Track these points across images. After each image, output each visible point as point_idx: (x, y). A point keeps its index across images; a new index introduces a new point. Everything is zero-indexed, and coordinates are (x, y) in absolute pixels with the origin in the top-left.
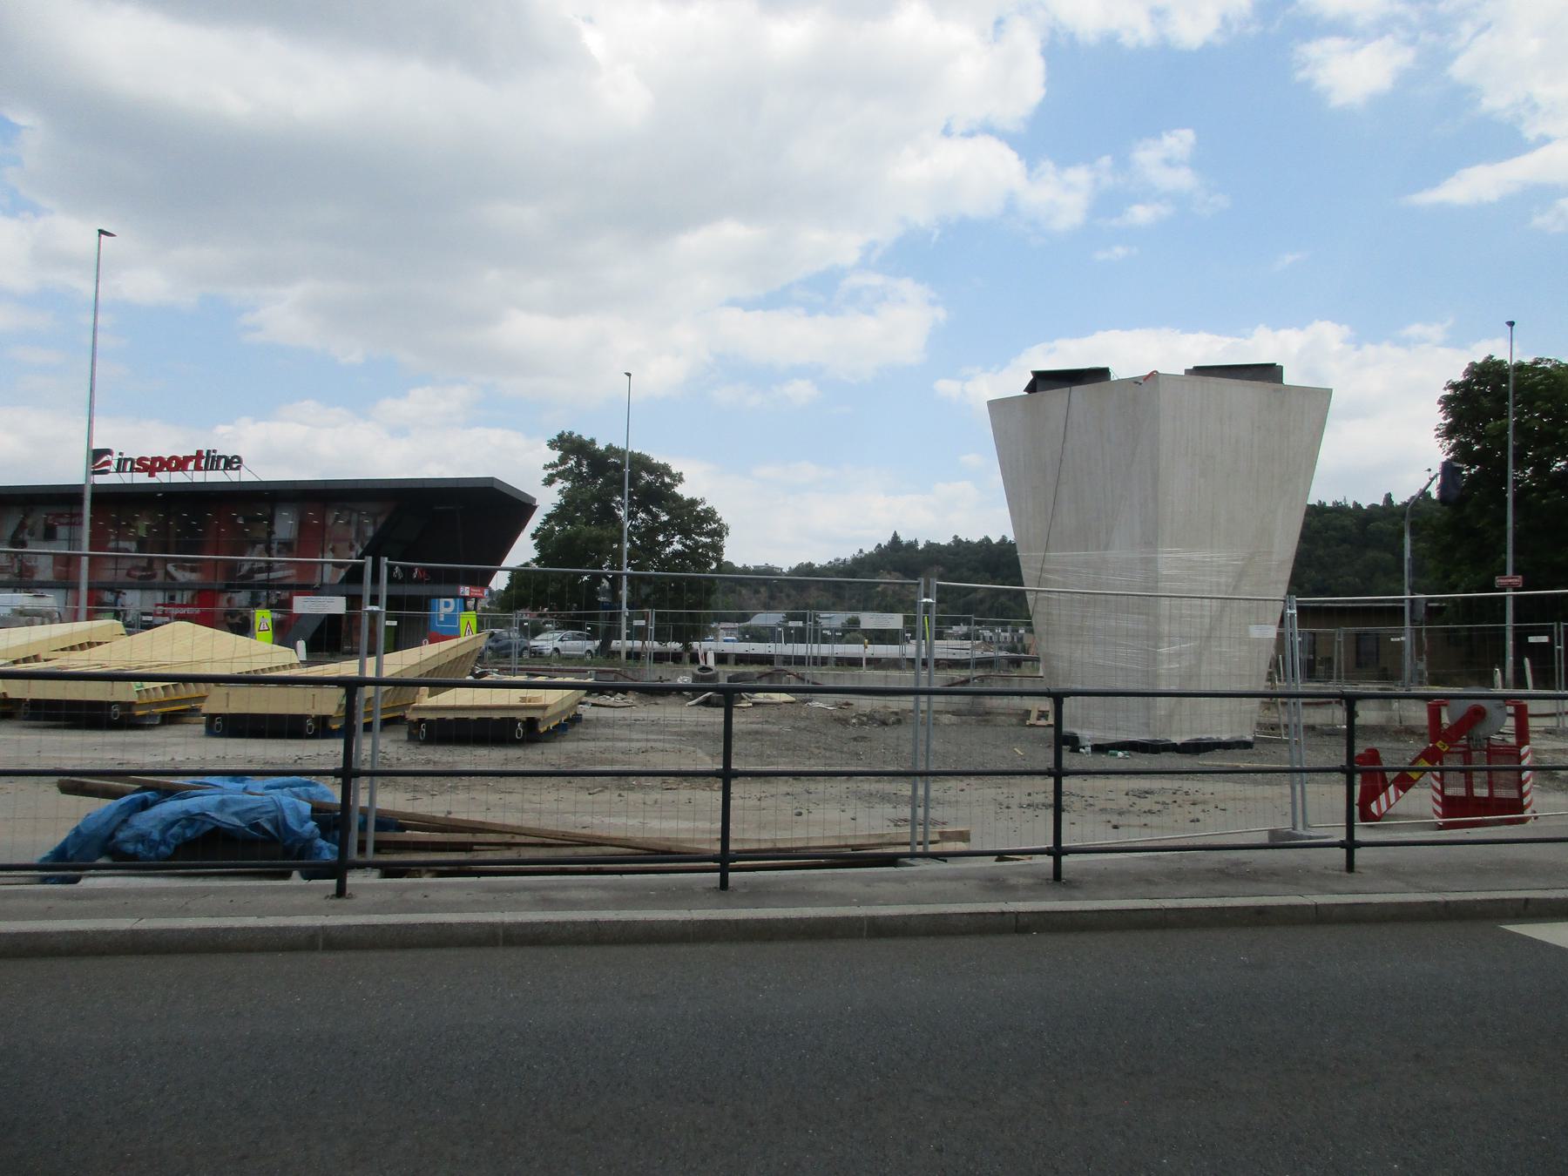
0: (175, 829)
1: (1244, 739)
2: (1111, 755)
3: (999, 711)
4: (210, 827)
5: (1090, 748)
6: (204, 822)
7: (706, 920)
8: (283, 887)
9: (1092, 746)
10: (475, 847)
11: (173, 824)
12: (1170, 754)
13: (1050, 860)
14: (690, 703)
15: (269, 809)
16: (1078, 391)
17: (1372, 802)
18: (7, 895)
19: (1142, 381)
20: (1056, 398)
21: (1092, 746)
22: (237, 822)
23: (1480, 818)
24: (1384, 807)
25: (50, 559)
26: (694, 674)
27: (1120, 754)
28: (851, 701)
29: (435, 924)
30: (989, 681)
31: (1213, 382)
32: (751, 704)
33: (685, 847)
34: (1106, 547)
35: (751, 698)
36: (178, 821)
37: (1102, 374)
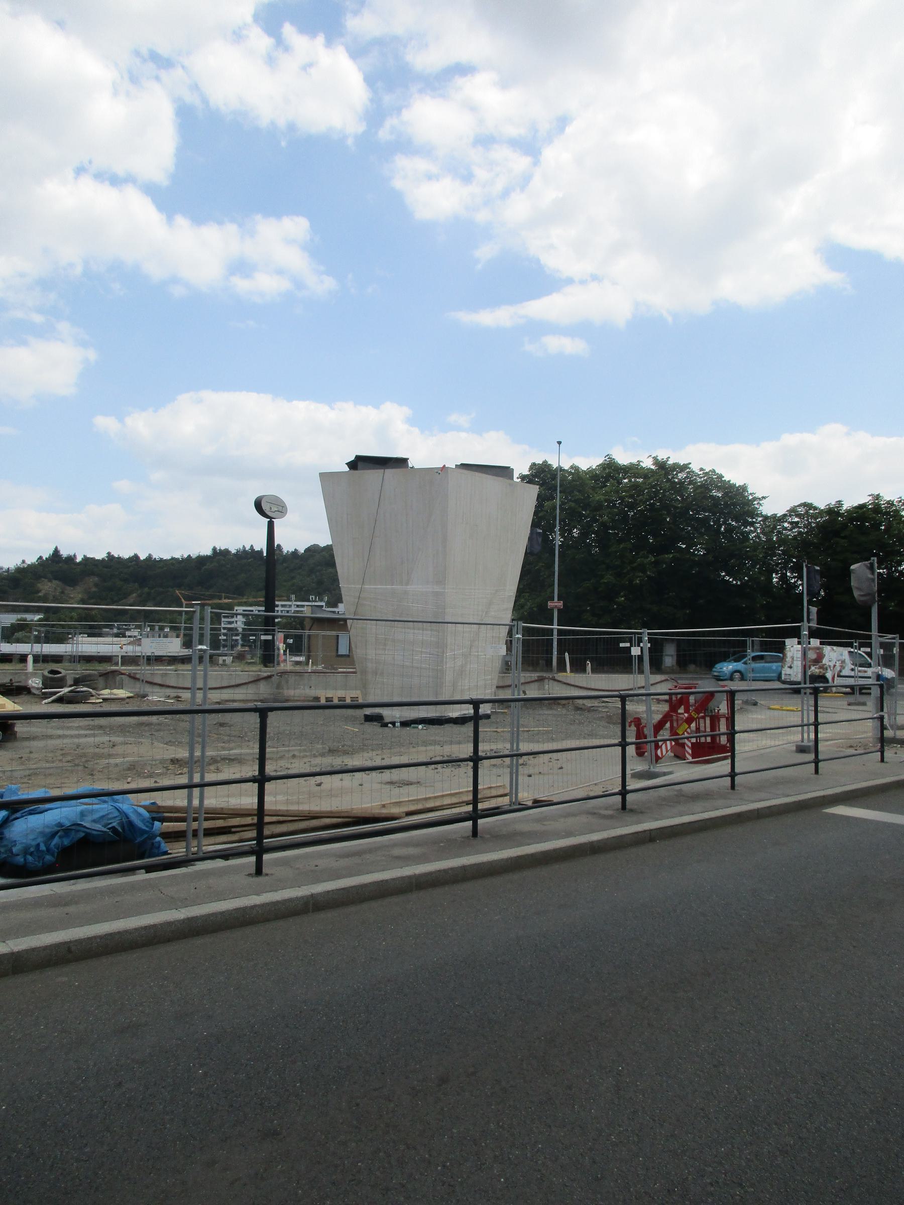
0: (56, 840)
1: (486, 713)
2: (414, 728)
3: (296, 698)
4: (82, 835)
5: (399, 724)
6: (78, 831)
7: (517, 857)
8: (184, 875)
9: (400, 722)
10: (233, 830)
11: (53, 835)
12: (451, 725)
13: (619, 798)
14: (46, 701)
15: (115, 815)
16: (389, 473)
17: (692, 752)
18: (6, 907)
19: (440, 472)
20: (373, 476)
21: (400, 722)
22: (98, 827)
23: (719, 756)
24: (664, 753)
25: (158, 627)
26: (44, 676)
27: (420, 727)
28: (180, 695)
29: (378, 882)
30: (286, 676)
31: (478, 475)
32: (101, 701)
33: (383, 813)
34: (407, 584)
35: (99, 695)
36: (57, 832)
37: (401, 462)
